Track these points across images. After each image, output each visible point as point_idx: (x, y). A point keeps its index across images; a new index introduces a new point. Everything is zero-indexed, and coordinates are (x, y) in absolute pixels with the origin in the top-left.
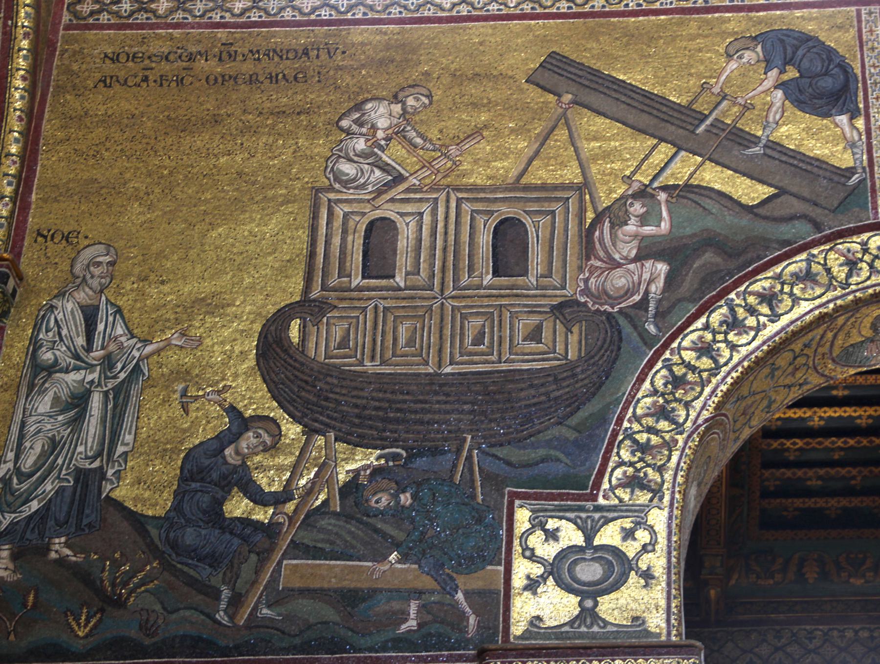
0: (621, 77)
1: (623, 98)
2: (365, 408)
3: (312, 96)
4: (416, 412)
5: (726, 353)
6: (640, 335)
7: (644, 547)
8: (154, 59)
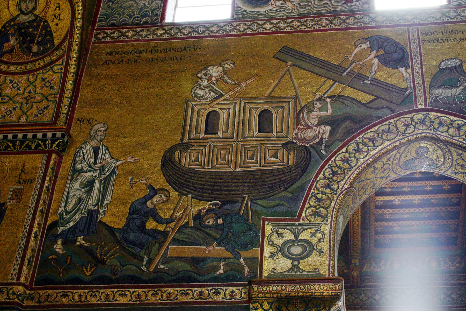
0: (312, 55)
1: (313, 63)
2: (204, 185)
3: (187, 65)
4: (225, 186)
5: (355, 162)
6: (319, 155)
7: (319, 240)
8: (126, 53)
